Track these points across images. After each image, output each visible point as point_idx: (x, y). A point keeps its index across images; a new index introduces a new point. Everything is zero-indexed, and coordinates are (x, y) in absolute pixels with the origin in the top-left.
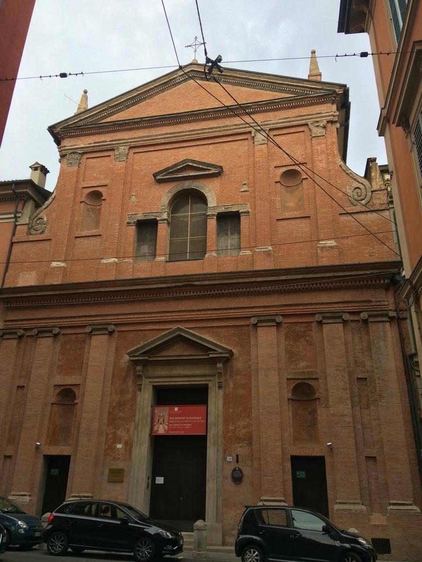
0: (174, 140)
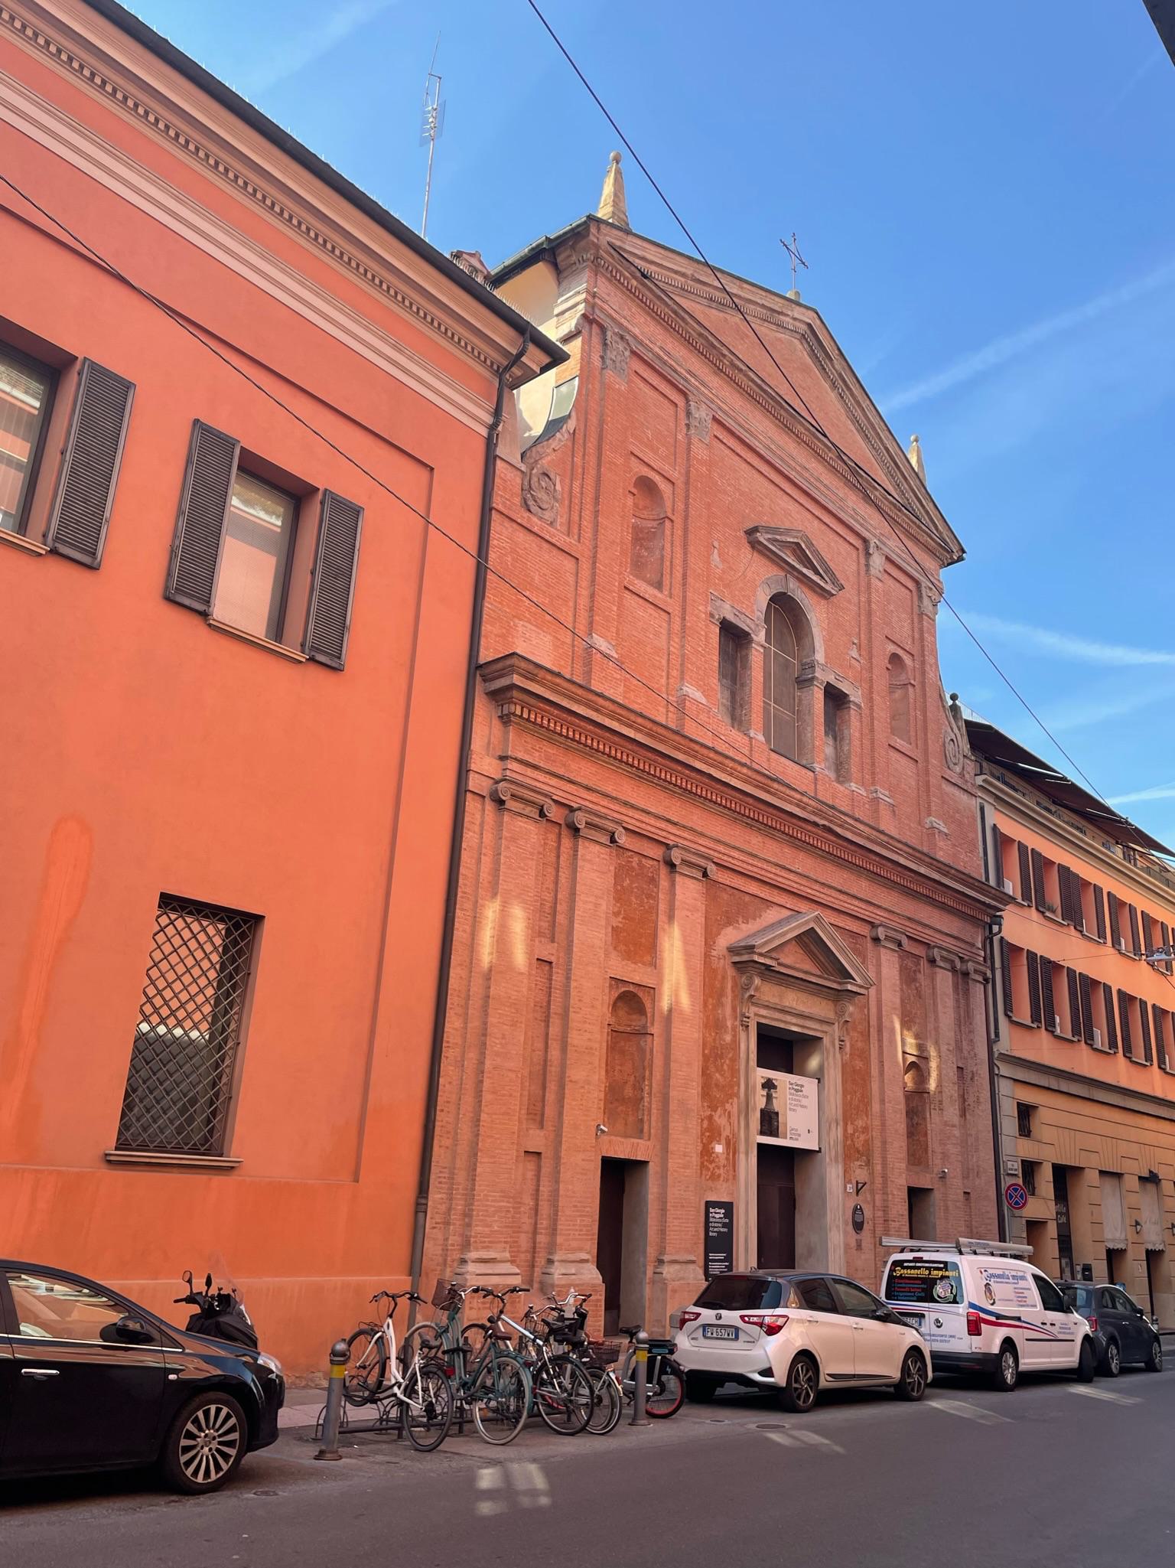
0: (778, 463)
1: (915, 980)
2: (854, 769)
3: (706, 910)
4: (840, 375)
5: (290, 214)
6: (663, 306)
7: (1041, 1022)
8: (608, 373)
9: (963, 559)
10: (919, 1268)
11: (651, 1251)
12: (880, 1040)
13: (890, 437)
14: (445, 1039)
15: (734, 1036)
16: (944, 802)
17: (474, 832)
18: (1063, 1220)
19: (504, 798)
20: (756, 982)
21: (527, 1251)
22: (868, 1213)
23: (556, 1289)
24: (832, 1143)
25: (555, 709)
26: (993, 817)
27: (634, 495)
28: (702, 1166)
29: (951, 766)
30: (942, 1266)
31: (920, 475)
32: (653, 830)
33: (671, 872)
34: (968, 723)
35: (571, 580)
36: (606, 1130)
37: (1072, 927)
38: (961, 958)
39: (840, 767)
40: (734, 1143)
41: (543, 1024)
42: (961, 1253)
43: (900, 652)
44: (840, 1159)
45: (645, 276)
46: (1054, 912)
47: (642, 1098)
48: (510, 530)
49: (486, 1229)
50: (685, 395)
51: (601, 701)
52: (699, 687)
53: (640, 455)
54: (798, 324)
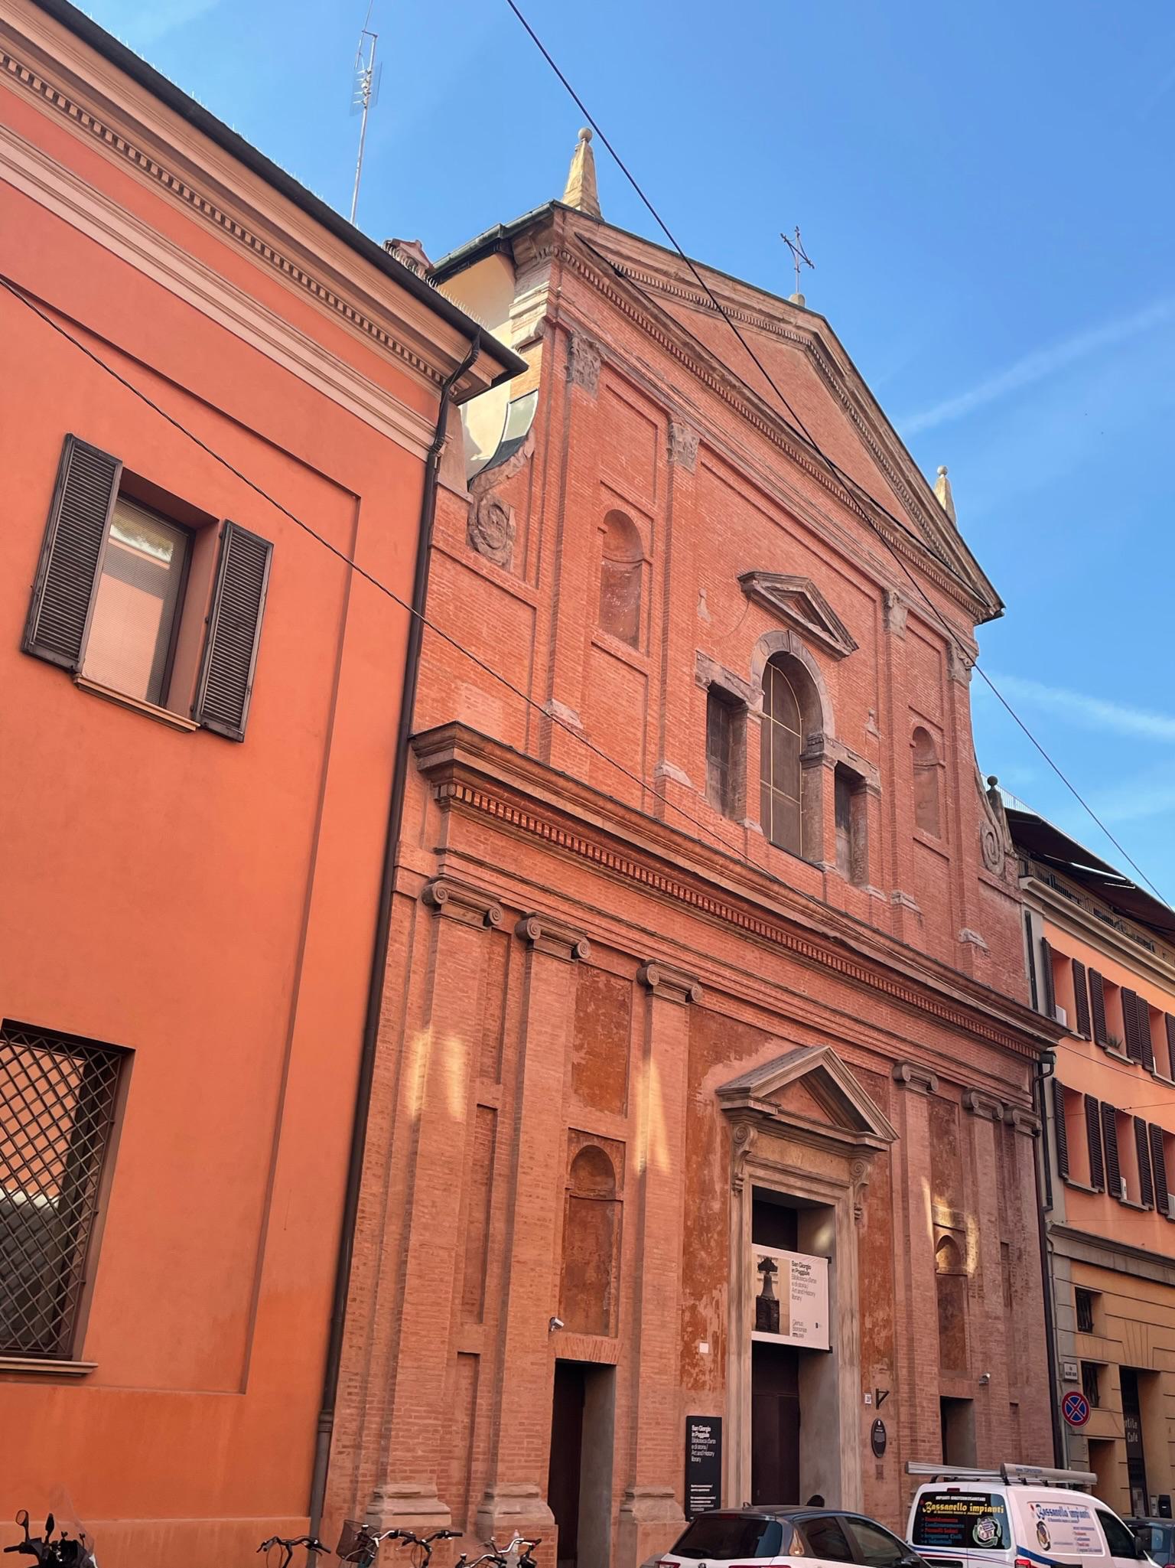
1: (947, 1132)
2: (871, 868)
3: (690, 1045)
4: (853, 394)
5: (252, 238)
6: (640, 310)
7: (1103, 1186)
8: (574, 387)
9: (1001, 615)
10: (955, 1502)
11: (617, 1483)
12: (906, 1209)
13: (913, 469)
14: (360, 1207)
15: (724, 1203)
16: (981, 910)
17: (402, 944)
18: (1134, 1438)
19: (440, 901)
20: (752, 1134)
21: (458, 1483)
22: (891, 1430)
23: (496, 1533)
24: (846, 1339)
25: (505, 791)
26: (1042, 929)
27: (604, 532)
28: (683, 1371)
29: (990, 865)
30: (983, 1499)
31: (949, 513)
32: (625, 942)
33: (647, 995)
34: (1009, 812)
35: (527, 633)
36: (562, 1324)
37: (1140, 1066)
38: (1004, 1105)
39: (855, 865)
40: (723, 1342)
41: (483, 1189)
42: (1007, 1483)
43: (927, 726)
44: (856, 1362)
45: (620, 275)
46: (1117, 1047)
47: (608, 1283)
48: (453, 572)
49: (409, 1454)
50: (667, 415)
51: (561, 782)
52: (682, 766)
53: (613, 486)
54: (801, 333)
